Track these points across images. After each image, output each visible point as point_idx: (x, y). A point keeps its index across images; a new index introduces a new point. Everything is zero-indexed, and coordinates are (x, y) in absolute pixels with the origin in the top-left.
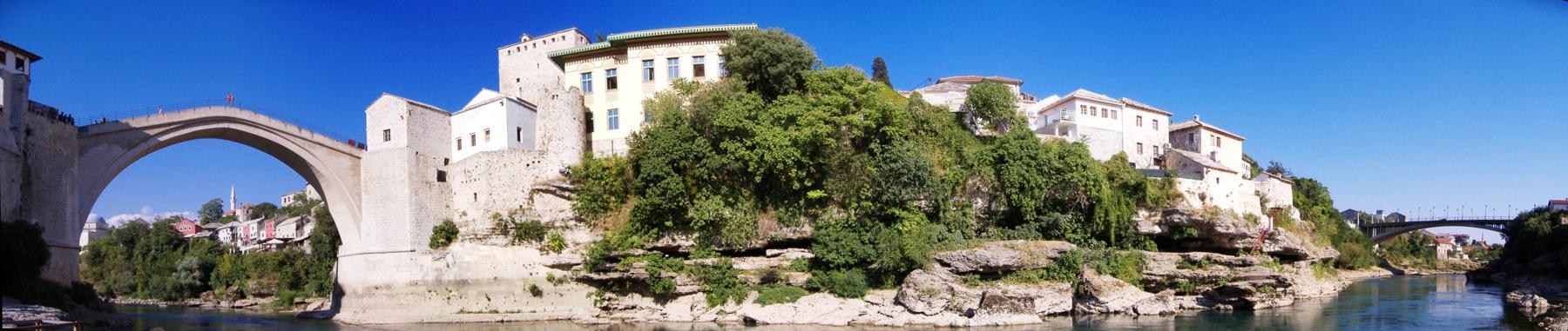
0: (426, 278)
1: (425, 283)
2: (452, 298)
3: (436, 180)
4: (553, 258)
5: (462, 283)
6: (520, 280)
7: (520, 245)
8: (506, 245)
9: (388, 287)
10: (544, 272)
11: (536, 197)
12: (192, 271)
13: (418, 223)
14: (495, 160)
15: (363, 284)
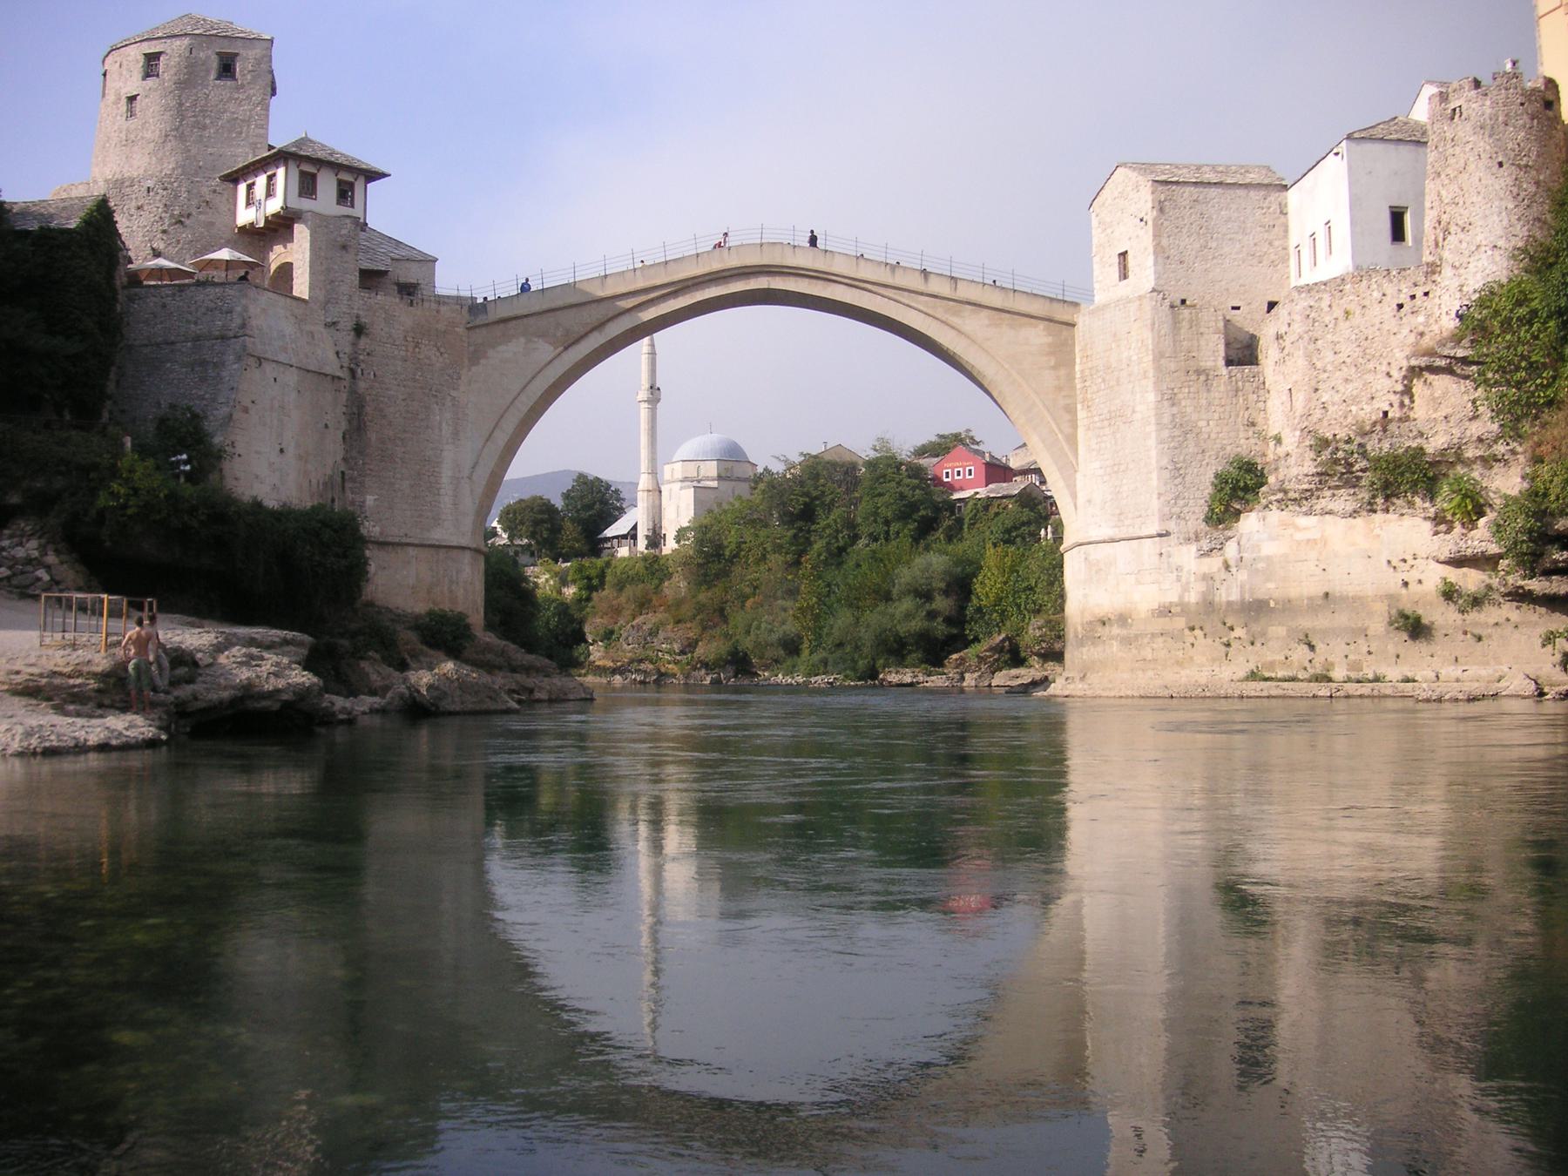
0: (1186, 599)
1: (1184, 608)
2: (1235, 644)
3: (1221, 362)
4: (1449, 543)
5: (1256, 609)
6: (1381, 598)
7: (1387, 511)
8: (1354, 514)
9: (1123, 619)
10: (1434, 576)
11: (1418, 387)
12: (927, 596)
13: (1177, 471)
14: (1325, 304)
15: (1082, 613)
